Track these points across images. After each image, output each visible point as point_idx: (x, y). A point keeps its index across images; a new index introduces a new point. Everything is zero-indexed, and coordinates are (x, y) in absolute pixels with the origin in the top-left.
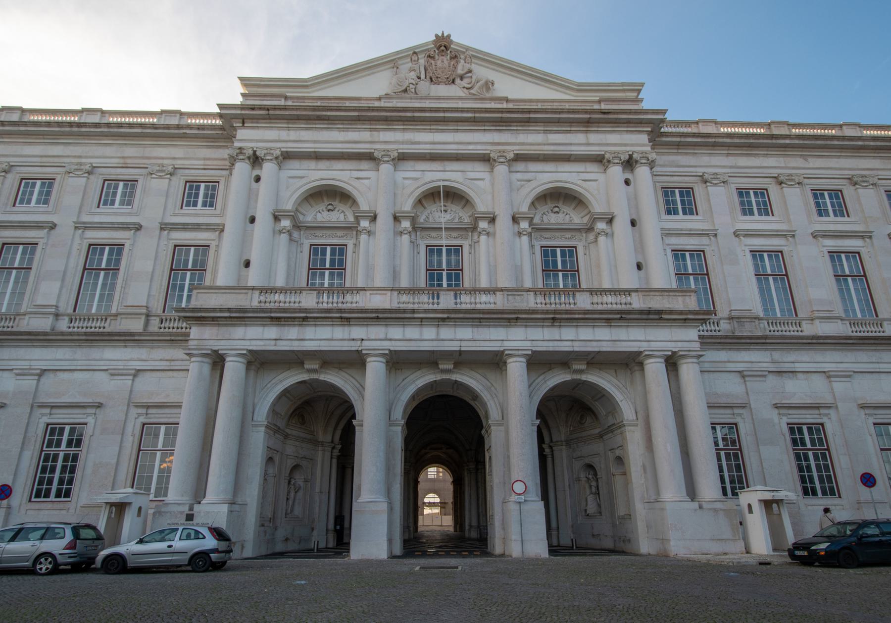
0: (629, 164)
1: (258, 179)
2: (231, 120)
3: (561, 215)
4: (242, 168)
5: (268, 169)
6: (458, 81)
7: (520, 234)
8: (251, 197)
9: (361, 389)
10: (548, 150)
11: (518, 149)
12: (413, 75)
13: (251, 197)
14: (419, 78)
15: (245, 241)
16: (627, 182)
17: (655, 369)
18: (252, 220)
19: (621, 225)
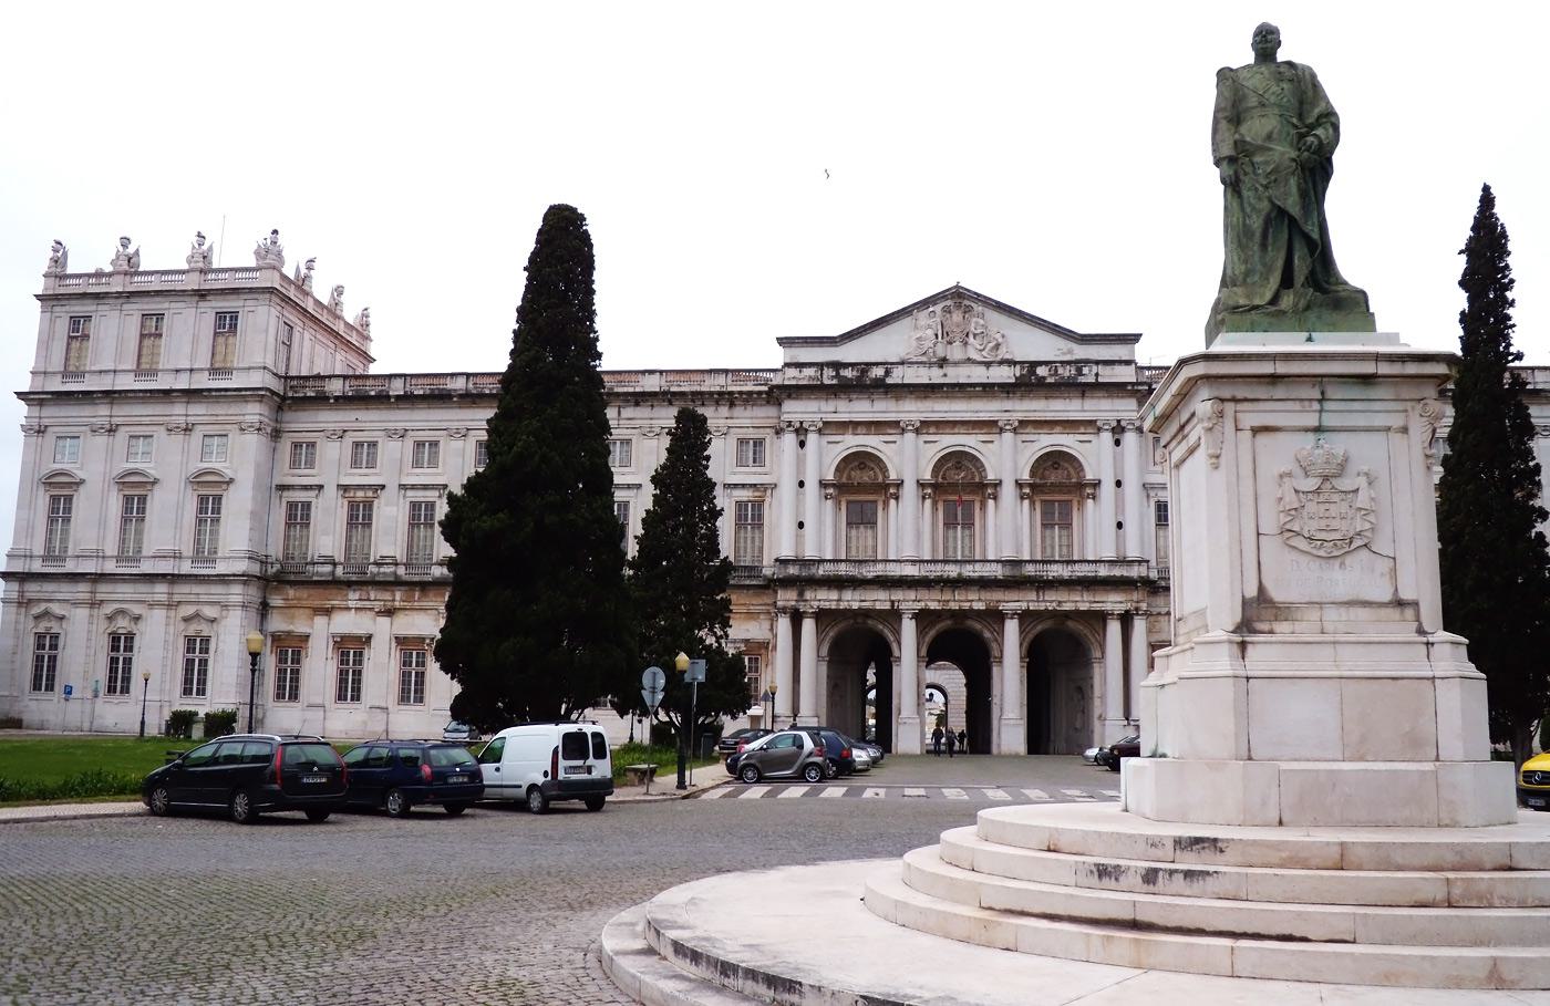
0: (1118, 430)
1: (802, 444)
2: (776, 395)
3: (1060, 471)
4: (789, 439)
5: (812, 438)
6: (971, 336)
7: (1022, 498)
8: (800, 463)
9: (897, 633)
10: (1049, 416)
11: (1021, 416)
12: (930, 332)
13: (800, 463)
14: (937, 335)
15: (799, 503)
16: (1117, 443)
17: (1114, 628)
18: (801, 484)
19: (1107, 488)
